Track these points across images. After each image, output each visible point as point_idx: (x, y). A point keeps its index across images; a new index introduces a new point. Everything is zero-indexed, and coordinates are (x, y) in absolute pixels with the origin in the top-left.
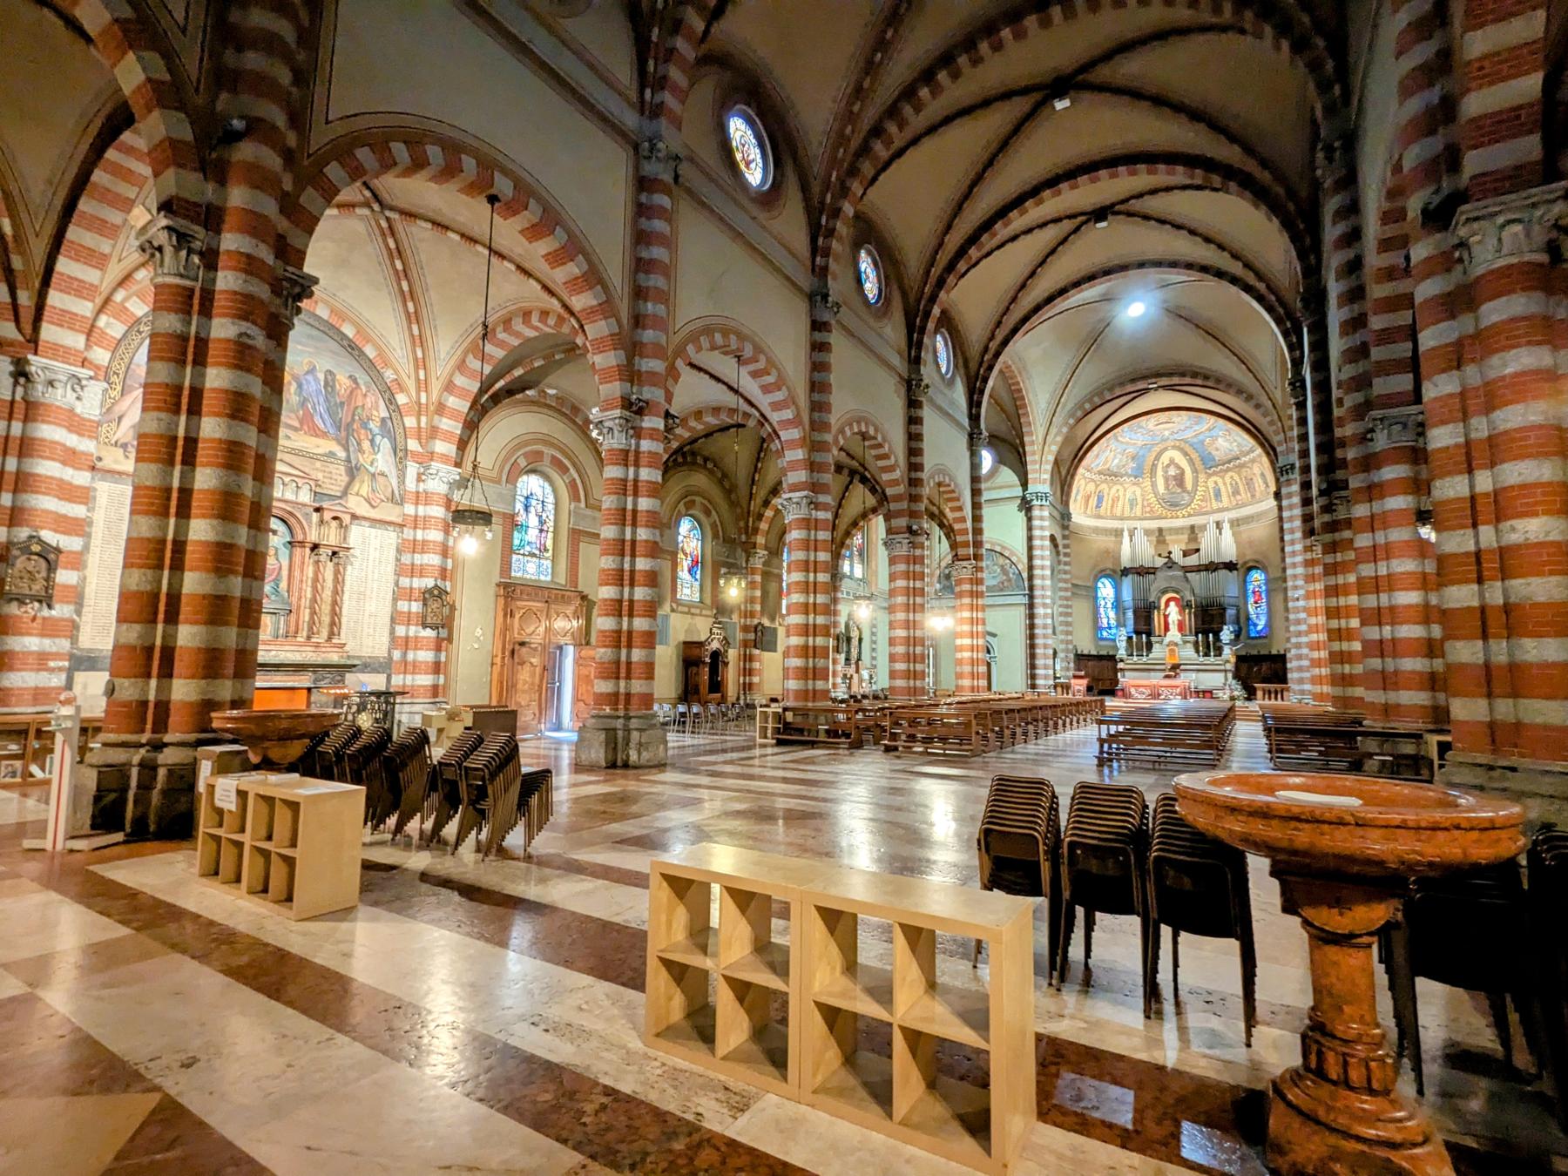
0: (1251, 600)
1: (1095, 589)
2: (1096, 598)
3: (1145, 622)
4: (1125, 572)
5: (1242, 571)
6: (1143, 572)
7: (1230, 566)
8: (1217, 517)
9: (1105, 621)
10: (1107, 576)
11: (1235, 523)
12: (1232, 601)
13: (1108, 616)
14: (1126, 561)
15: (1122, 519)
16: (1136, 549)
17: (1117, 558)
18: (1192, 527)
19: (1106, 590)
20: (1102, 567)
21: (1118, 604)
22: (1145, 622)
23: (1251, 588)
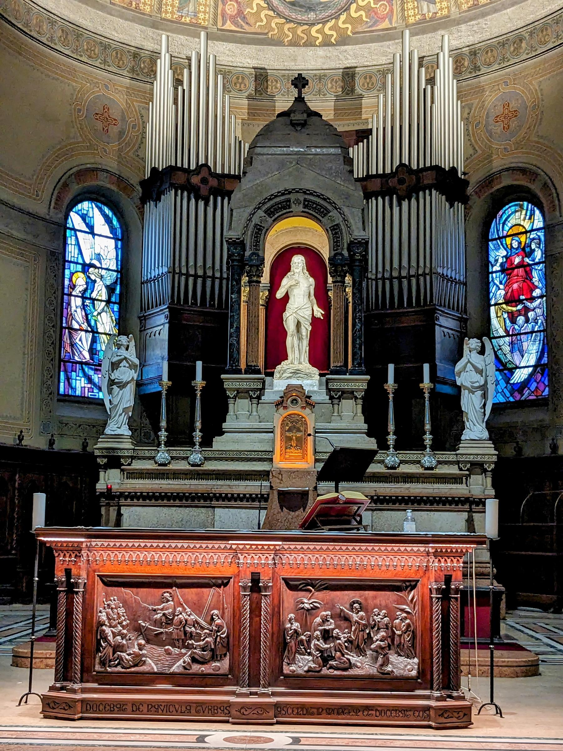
0: (498, 293)
1: (60, 230)
2: (57, 259)
3: (205, 346)
4: (156, 184)
5: (478, 205)
6: (206, 185)
7: (449, 183)
8: (415, 45)
9: (83, 341)
10: (98, 196)
11: (468, 63)
12: (456, 294)
13: (93, 322)
14: (158, 151)
15: (156, 24)
16: (193, 109)
17: (135, 136)
18: (349, 75)
19: (93, 240)
20: (87, 160)
21: (126, 292)
22: (205, 346)
23: (498, 255)
